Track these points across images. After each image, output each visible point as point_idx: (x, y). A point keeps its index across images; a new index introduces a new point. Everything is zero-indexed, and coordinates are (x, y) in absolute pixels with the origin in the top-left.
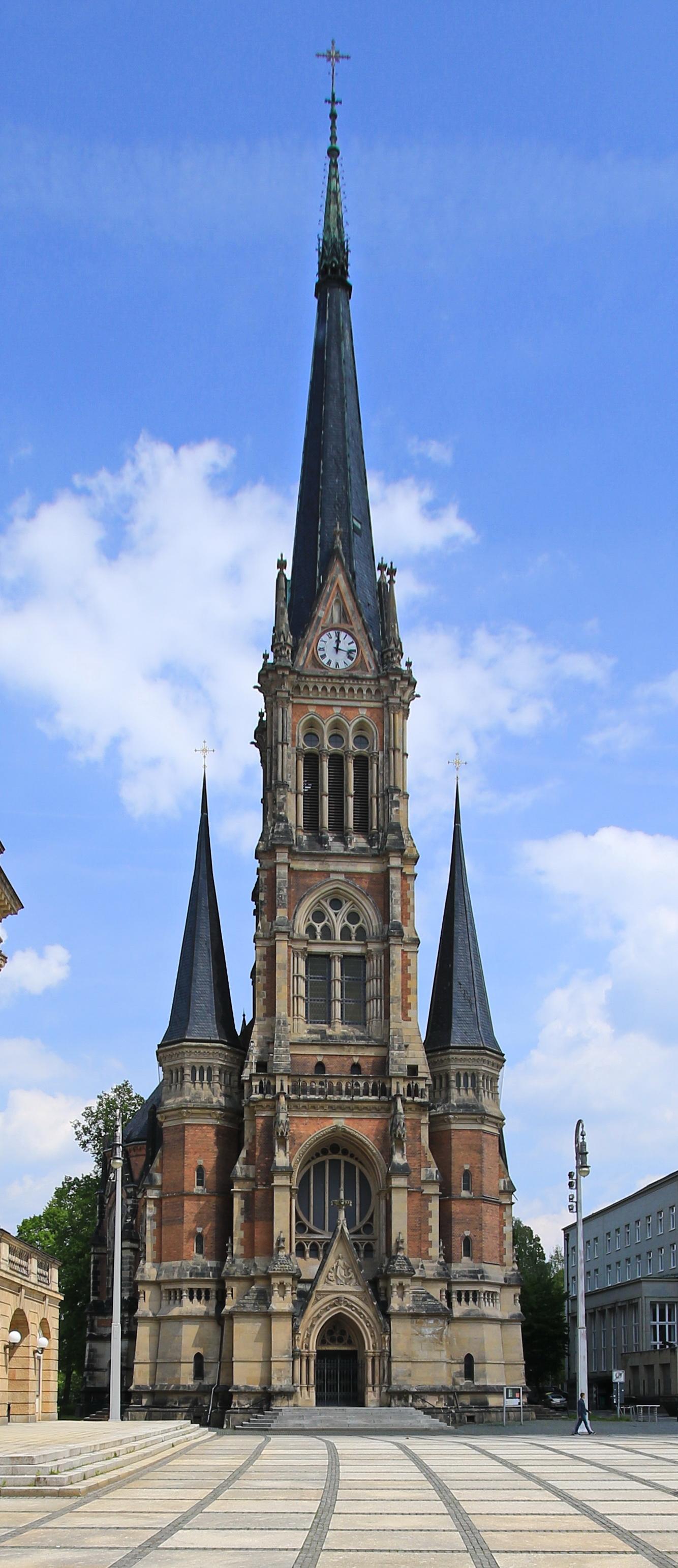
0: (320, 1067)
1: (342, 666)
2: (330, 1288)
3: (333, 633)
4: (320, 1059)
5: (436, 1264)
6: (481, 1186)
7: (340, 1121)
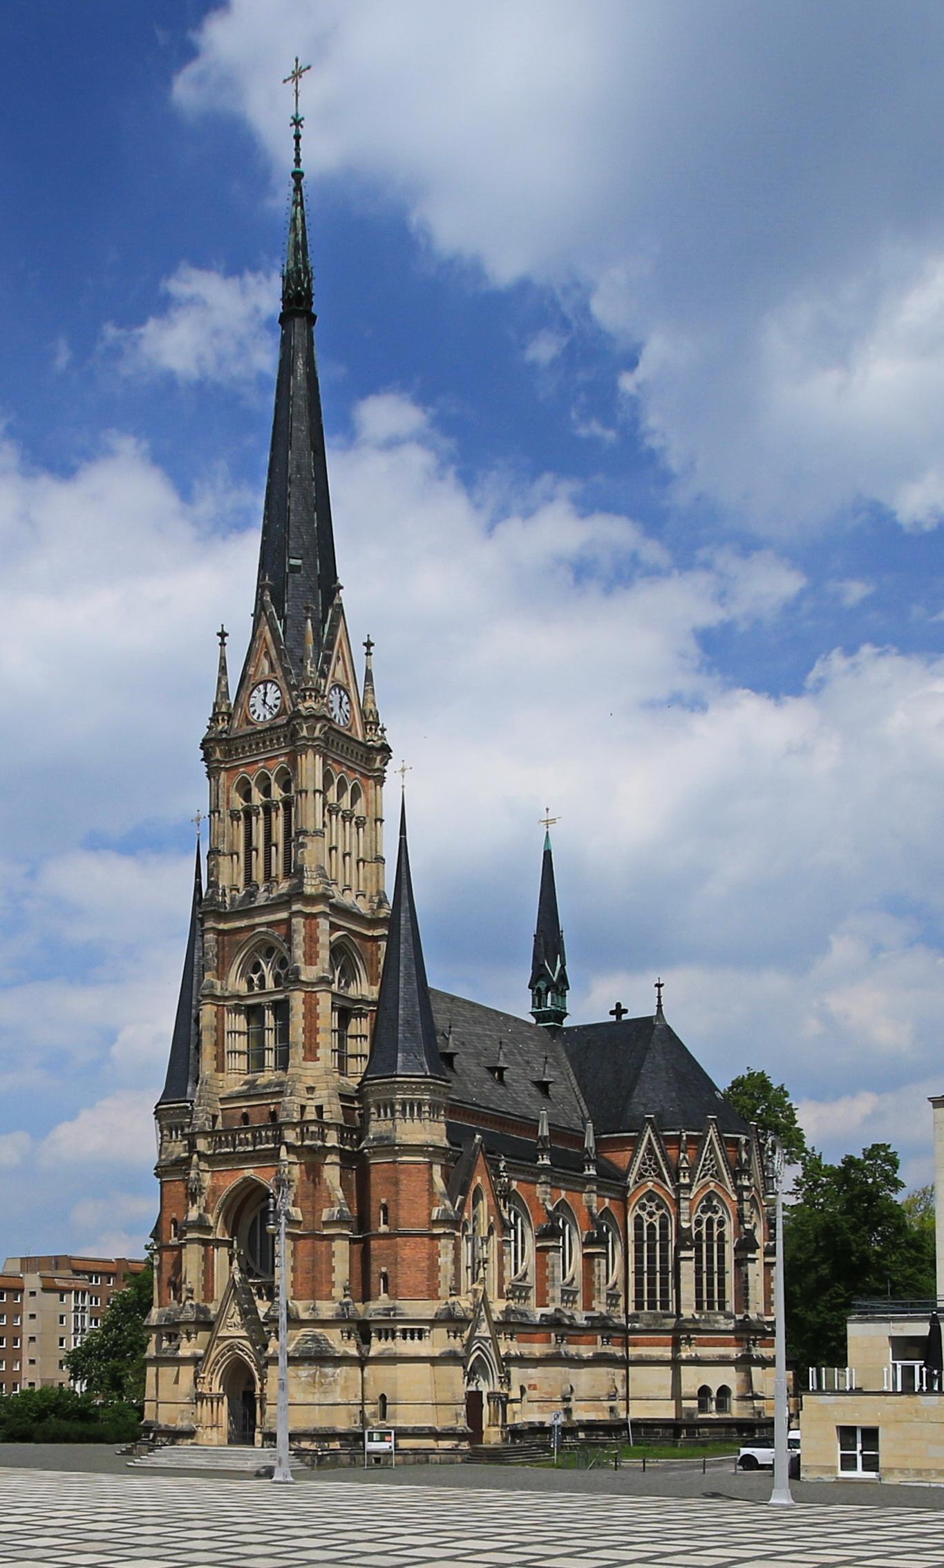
0: (245, 1118)
1: (269, 717)
2: (228, 1334)
3: (261, 687)
4: (244, 1110)
5: (337, 1305)
6: (397, 1220)
7: (249, 1173)
